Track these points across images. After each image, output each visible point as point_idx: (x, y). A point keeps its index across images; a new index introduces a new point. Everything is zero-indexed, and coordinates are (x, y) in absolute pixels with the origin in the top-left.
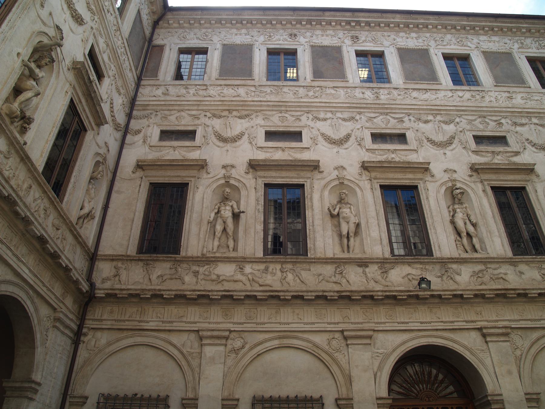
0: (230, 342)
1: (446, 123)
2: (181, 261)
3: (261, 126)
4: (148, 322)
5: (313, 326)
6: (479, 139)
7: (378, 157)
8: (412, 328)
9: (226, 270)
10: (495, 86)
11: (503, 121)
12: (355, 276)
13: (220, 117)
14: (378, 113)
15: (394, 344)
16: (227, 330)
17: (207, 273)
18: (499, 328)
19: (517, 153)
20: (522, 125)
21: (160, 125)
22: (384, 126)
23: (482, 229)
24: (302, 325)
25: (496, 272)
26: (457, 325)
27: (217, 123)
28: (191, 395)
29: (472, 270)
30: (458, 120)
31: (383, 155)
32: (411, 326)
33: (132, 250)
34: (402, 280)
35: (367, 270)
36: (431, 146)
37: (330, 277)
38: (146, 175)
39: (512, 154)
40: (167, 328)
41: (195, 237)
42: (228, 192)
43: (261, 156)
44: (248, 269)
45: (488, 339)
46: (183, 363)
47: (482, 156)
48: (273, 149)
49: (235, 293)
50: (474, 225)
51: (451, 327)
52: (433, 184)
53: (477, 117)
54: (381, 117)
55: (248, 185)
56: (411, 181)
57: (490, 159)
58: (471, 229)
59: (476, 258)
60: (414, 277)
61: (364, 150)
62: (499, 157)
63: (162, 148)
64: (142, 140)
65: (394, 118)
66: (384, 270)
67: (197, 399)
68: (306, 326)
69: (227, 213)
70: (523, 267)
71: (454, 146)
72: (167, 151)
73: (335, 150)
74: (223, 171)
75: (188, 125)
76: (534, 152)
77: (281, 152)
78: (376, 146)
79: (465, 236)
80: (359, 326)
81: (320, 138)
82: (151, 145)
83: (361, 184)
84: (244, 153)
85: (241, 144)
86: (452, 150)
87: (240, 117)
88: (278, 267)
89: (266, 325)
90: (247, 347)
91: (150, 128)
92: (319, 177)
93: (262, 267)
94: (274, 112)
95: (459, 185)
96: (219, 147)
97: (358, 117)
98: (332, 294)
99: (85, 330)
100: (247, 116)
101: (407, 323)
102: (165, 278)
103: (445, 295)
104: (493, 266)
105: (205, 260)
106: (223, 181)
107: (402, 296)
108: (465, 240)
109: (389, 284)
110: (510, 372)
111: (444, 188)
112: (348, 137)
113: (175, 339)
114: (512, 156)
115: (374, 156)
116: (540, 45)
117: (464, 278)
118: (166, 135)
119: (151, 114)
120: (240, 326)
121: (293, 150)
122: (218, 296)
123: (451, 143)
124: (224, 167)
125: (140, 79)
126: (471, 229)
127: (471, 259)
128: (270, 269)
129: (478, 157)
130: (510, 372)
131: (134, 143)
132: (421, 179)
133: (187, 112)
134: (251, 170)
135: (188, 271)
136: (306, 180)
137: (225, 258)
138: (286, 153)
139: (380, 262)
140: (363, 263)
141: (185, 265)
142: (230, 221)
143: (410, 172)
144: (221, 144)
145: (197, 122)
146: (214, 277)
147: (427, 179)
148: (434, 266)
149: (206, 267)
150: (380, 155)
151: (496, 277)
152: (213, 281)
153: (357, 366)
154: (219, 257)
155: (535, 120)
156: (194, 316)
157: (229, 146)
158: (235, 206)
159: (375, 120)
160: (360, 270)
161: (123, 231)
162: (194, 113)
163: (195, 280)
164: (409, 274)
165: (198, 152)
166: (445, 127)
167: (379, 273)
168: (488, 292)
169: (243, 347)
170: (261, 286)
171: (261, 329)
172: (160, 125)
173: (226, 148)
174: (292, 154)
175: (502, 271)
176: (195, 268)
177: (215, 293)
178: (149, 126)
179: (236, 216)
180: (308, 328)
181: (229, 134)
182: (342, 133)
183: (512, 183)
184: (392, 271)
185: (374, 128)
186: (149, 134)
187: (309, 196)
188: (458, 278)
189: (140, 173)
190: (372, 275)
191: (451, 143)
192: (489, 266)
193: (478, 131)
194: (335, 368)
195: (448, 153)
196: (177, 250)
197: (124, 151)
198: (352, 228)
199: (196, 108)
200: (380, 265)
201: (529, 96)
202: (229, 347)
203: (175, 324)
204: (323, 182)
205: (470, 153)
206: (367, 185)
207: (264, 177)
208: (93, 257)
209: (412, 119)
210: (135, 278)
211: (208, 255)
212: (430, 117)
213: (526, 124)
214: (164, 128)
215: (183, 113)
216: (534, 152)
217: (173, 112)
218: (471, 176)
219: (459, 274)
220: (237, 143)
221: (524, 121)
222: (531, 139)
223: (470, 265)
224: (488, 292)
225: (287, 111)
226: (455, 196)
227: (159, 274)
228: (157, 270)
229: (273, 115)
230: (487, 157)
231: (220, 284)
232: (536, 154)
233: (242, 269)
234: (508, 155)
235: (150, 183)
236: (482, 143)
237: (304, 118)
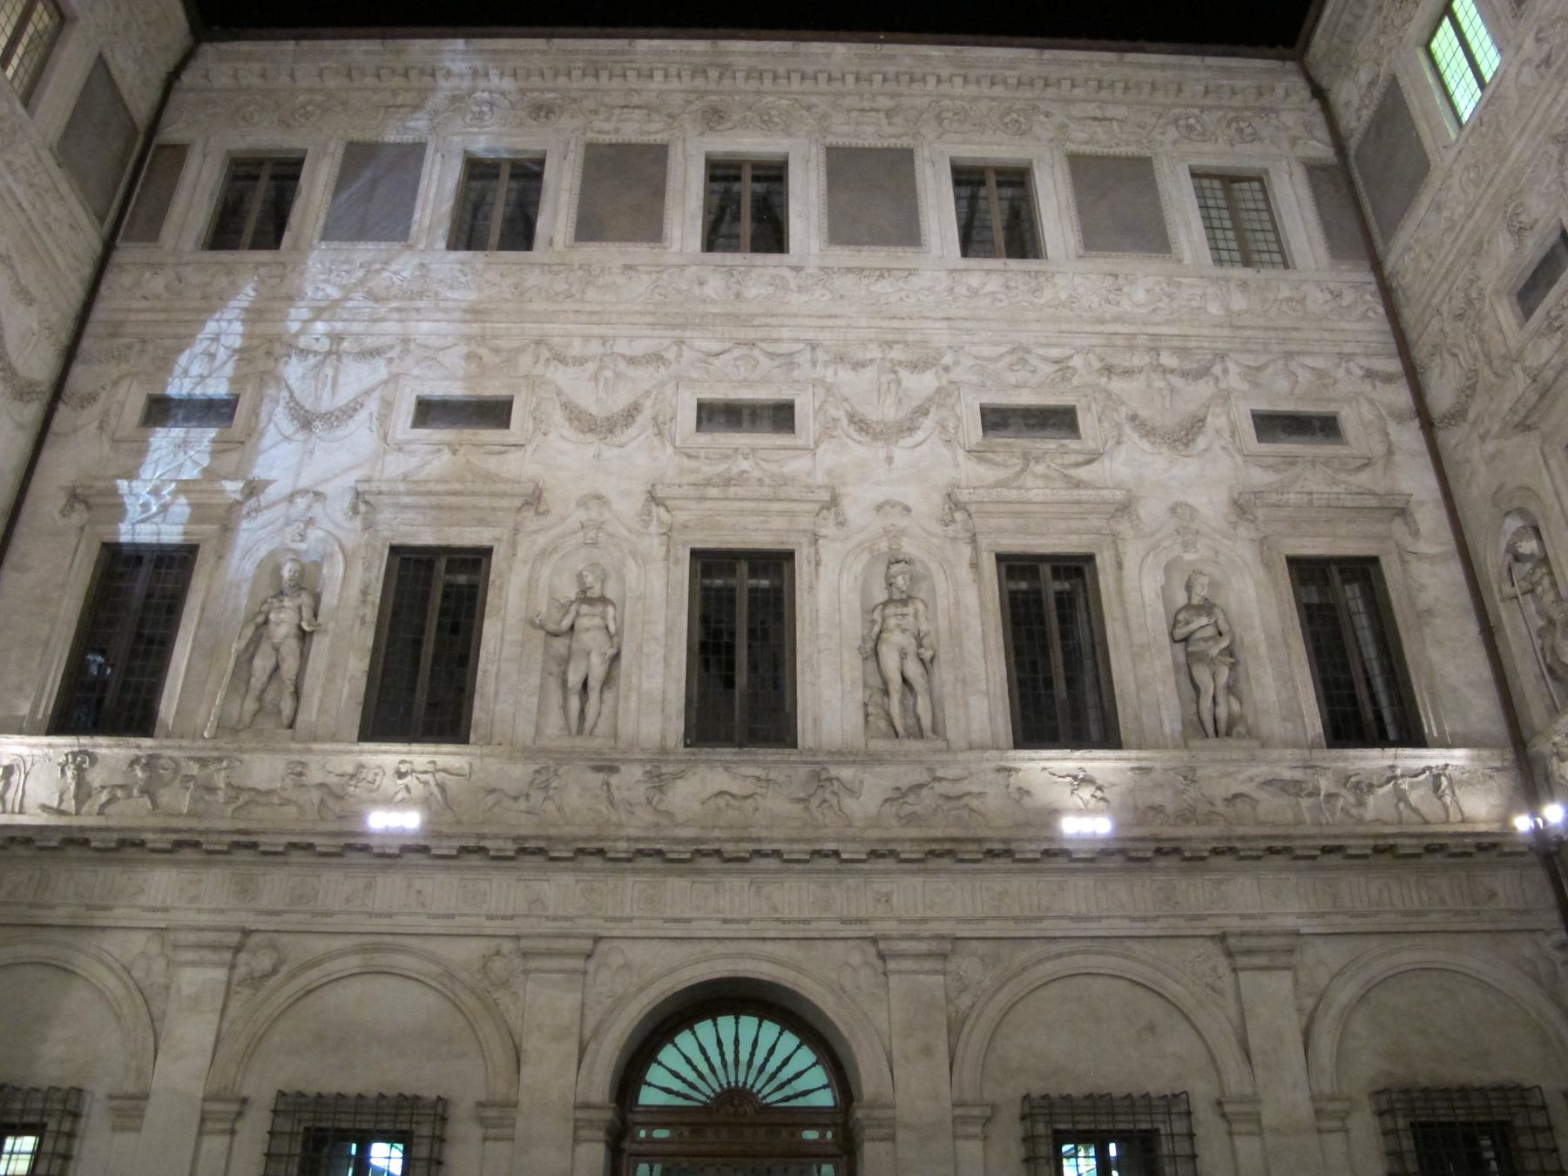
0: (243, 957)
1: (914, 366)
4: (52, 907)
11: (1077, 362)
12: (581, 796)
18: (921, 939)
20: (1128, 372)
23: (944, 674)
30: (948, 359)
35: (614, 780)
36: (855, 435)
45: (892, 965)
51: (801, 935)
54: (737, 352)
58: (914, 670)
64: (96, 424)
71: (920, 435)
73: (591, 451)
81: (558, 416)
82: (119, 435)
90: (284, 970)
97: (670, 355)
98: (500, 844)
101: (688, 921)
103: (791, 852)
110: (927, 1051)
112: (631, 413)
114: (1078, 465)
116: (1240, 131)
125: (109, 247)
126: (914, 670)
130: (927, 1051)
142: (291, 647)
155: (1169, 360)
159: (717, 362)
164: (721, 793)
169: (274, 971)
171: (322, 929)
180: (435, 926)
182: (621, 399)
184: (680, 783)
187: (498, 583)
188: (850, 804)
195: (900, 454)
197: (46, 456)
202: (241, 971)
212: (874, 352)
213: (1141, 370)
219: (853, 793)
222: (1144, 413)
230: (1005, 466)
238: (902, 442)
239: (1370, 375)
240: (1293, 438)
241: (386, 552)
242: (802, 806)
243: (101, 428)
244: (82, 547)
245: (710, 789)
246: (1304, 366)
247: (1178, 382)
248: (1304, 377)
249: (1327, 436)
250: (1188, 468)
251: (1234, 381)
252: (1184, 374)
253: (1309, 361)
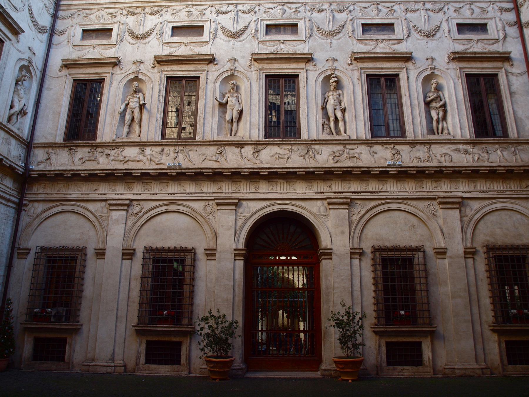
0: (131, 208)
2: (97, 147)
3: (168, 22)
4: (71, 194)
5: (193, 195)
6: (366, 27)
7: (269, 48)
8: (271, 197)
9: (131, 152)
11: (396, 8)
13: (134, 14)
14: (276, 3)
15: (254, 210)
16: (127, 200)
17: (116, 155)
19: (400, 41)
20: (415, 11)
21: (82, 25)
22: (280, 17)
24: (185, 195)
25: (351, 152)
26: (307, 196)
27: (131, 20)
28: (101, 246)
29: (331, 150)
30: (351, 8)
31: (273, 46)
32: (270, 196)
33: (60, 139)
34: (270, 158)
35: (243, 150)
37: (212, 157)
38: (70, 73)
39: (396, 42)
40: (85, 199)
41: (107, 127)
42: (135, 85)
43: (166, 51)
44: (148, 151)
46: (97, 224)
47: (366, 44)
48: (177, 44)
49: (133, 171)
50: (343, 111)
51: (302, 197)
52: (313, 72)
53: (370, 4)
55: (153, 79)
56: (294, 71)
57: (372, 47)
58: (339, 114)
59: (336, 140)
60: (280, 156)
61: (257, 42)
62: (381, 45)
63: (83, 47)
64: (67, 40)
65: (290, 8)
66: (256, 150)
67: (105, 249)
68: (188, 195)
69: (134, 104)
70: (377, 148)
71: (341, 35)
72: (88, 50)
74: (134, 67)
75: (106, 24)
76: (418, 39)
77: (185, 47)
78: (268, 38)
79: (331, 121)
80: (229, 195)
81: (220, 32)
83: (249, 74)
84: (155, 48)
85: (150, 41)
86: (338, 39)
87: (151, 14)
88: (172, 149)
89: (158, 195)
90: (143, 211)
91: (73, 28)
92: (213, 70)
93: (159, 149)
94: (182, 7)
95: (337, 73)
96: (131, 43)
98: (208, 171)
99: (24, 202)
100: (157, 12)
102: (84, 160)
104: (351, 147)
105: (115, 145)
106: (133, 76)
107: (264, 172)
108: (332, 124)
109: (258, 162)
110: (343, 233)
111: (323, 76)
113: (91, 206)
114: (394, 44)
115: (265, 47)
117: (324, 158)
118: (87, 33)
119: (74, 14)
120: (139, 196)
121: (194, 44)
122: (121, 173)
123: (338, 33)
124: (134, 63)
126: (339, 114)
127: (332, 140)
128: (165, 151)
129: (362, 46)
130: (343, 233)
131: (60, 43)
132: (303, 69)
133: (105, 10)
134: (157, 65)
135: (102, 154)
136: (202, 72)
137: (130, 142)
138: (188, 47)
139: (254, 144)
140: (240, 145)
141: (99, 149)
143: (294, 62)
144: (133, 41)
145: (115, 20)
146: (121, 158)
147: (308, 68)
148: (299, 147)
149: (116, 150)
150: (271, 46)
151: (350, 156)
152: (121, 161)
153: (222, 226)
154: (125, 142)
156: (105, 190)
157: (141, 43)
158: (141, 98)
159: (272, 11)
160: (237, 150)
161: (54, 122)
162: (111, 11)
163: (107, 160)
164: (277, 153)
165: (114, 50)
166: (338, 16)
167: (252, 153)
168: (336, 170)
169: (140, 211)
170: (157, 164)
171: (154, 198)
172: (82, 25)
173: (137, 45)
174: (193, 48)
175: (358, 151)
176: (107, 151)
177: (119, 172)
178: (72, 26)
179: (142, 107)
181: (140, 31)
183: (387, 70)
185: (270, 20)
186: (72, 34)
189: (65, 72)
190: (246, 154)
191: (338, 33)
192: (347, 146)
193: (368, 19)
194: (206, 227)
195: (334, 42)
196: (94, 137)
197: (52, 51)
198: (235, 114)
199: (113, 6)
200: (253, 146)
203: (90, 195)
204: (216, 74)
205: (355, 42)
206: (254, 75)
207: (167, 71)
208: (29, 145)
209: (308, 8)
210: (62, 161)
211: (117, 141)
212: (325, 6)
213: (418, 10)
214: (86, 28)
215: (102, 12)
216: (418, 39)
217: (93, 11)
218: (351, 64)
220: (147, 40)
221: (417, 7)
222: (418, 25)
223: (331, 146)
224: (336, 170)
225: (193, 5)
226: (332, 83)
227: (80, 157)
228: (78, 154)
229: (180, 10)
230: (370, 45)
231: (126, 164)
232: (419, 41)
233: (143, 151)
234: (391, 42)
235: (74, 80)
236: (370, 30)
237: (207, 12)
238: (335, 38)
240: (470, 32)
241: (166, 79)
242: (302, 157)
243: (68, 42)
244: (67, 81)
245: (273, 152)
246: (476, 6)
247: (431, 14)
248: (477, 11)
249: (483, 32)
250: (432, 44)
251: (451, 13)
252: (433, 11)
253: (478, 4)
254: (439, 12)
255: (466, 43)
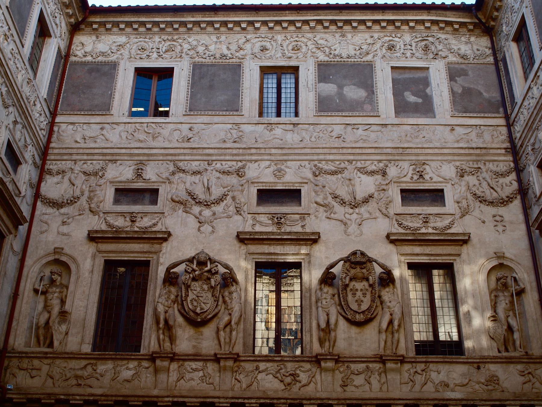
10: (7, 7)
201: (16, 55)
239: (34, 155)
254: (5, 108)
255: (5, 173)
